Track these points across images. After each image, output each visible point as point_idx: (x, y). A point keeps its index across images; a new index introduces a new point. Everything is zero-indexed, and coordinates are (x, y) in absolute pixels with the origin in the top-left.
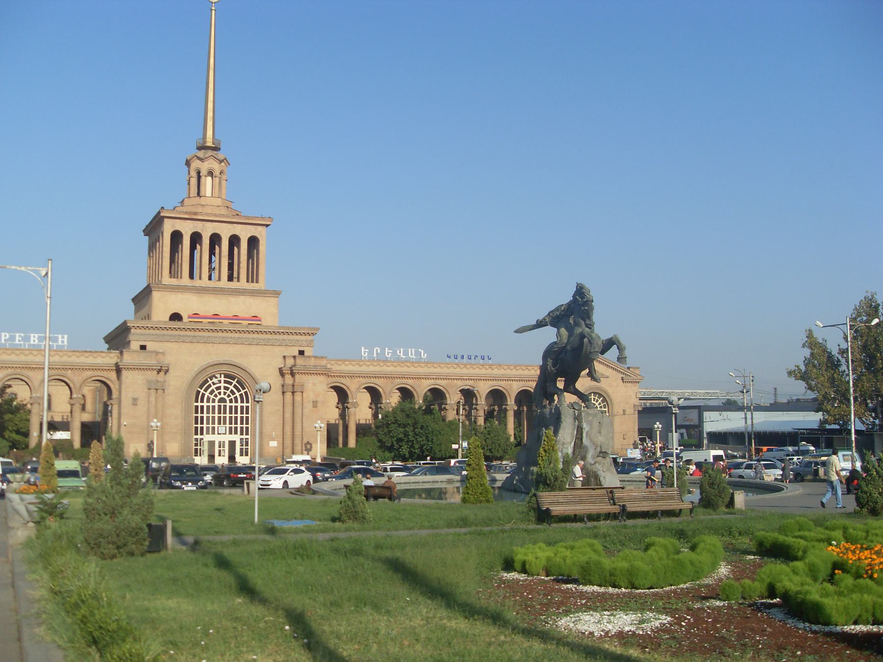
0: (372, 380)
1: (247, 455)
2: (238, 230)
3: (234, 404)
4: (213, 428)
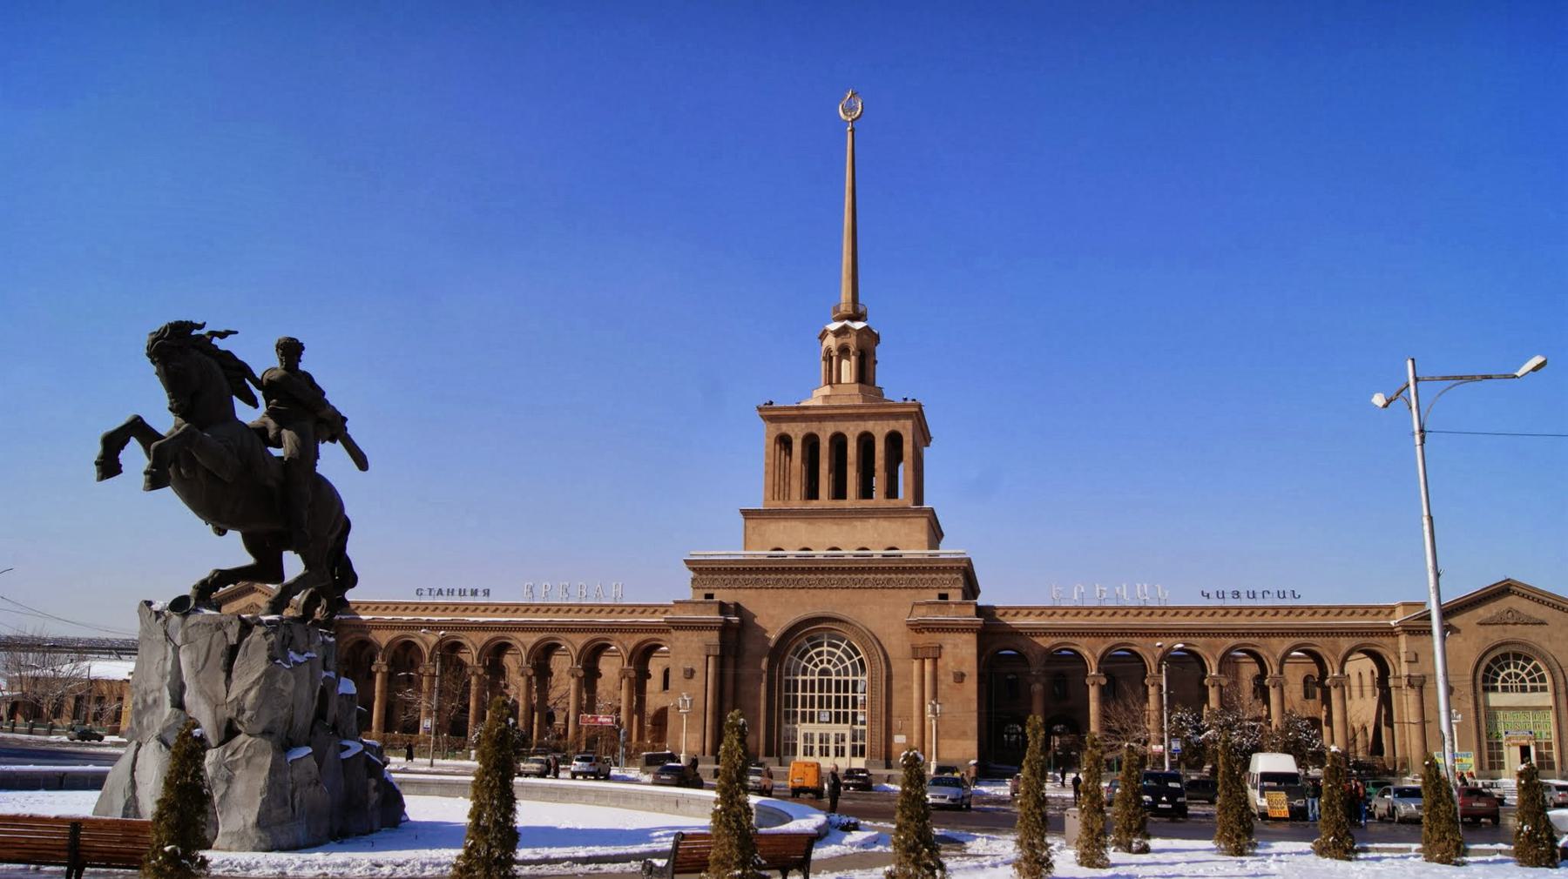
0: (1069, 640)
1: (862, 754)
2: (869, 426)
3: (842, 678)
4: (812, 714)
